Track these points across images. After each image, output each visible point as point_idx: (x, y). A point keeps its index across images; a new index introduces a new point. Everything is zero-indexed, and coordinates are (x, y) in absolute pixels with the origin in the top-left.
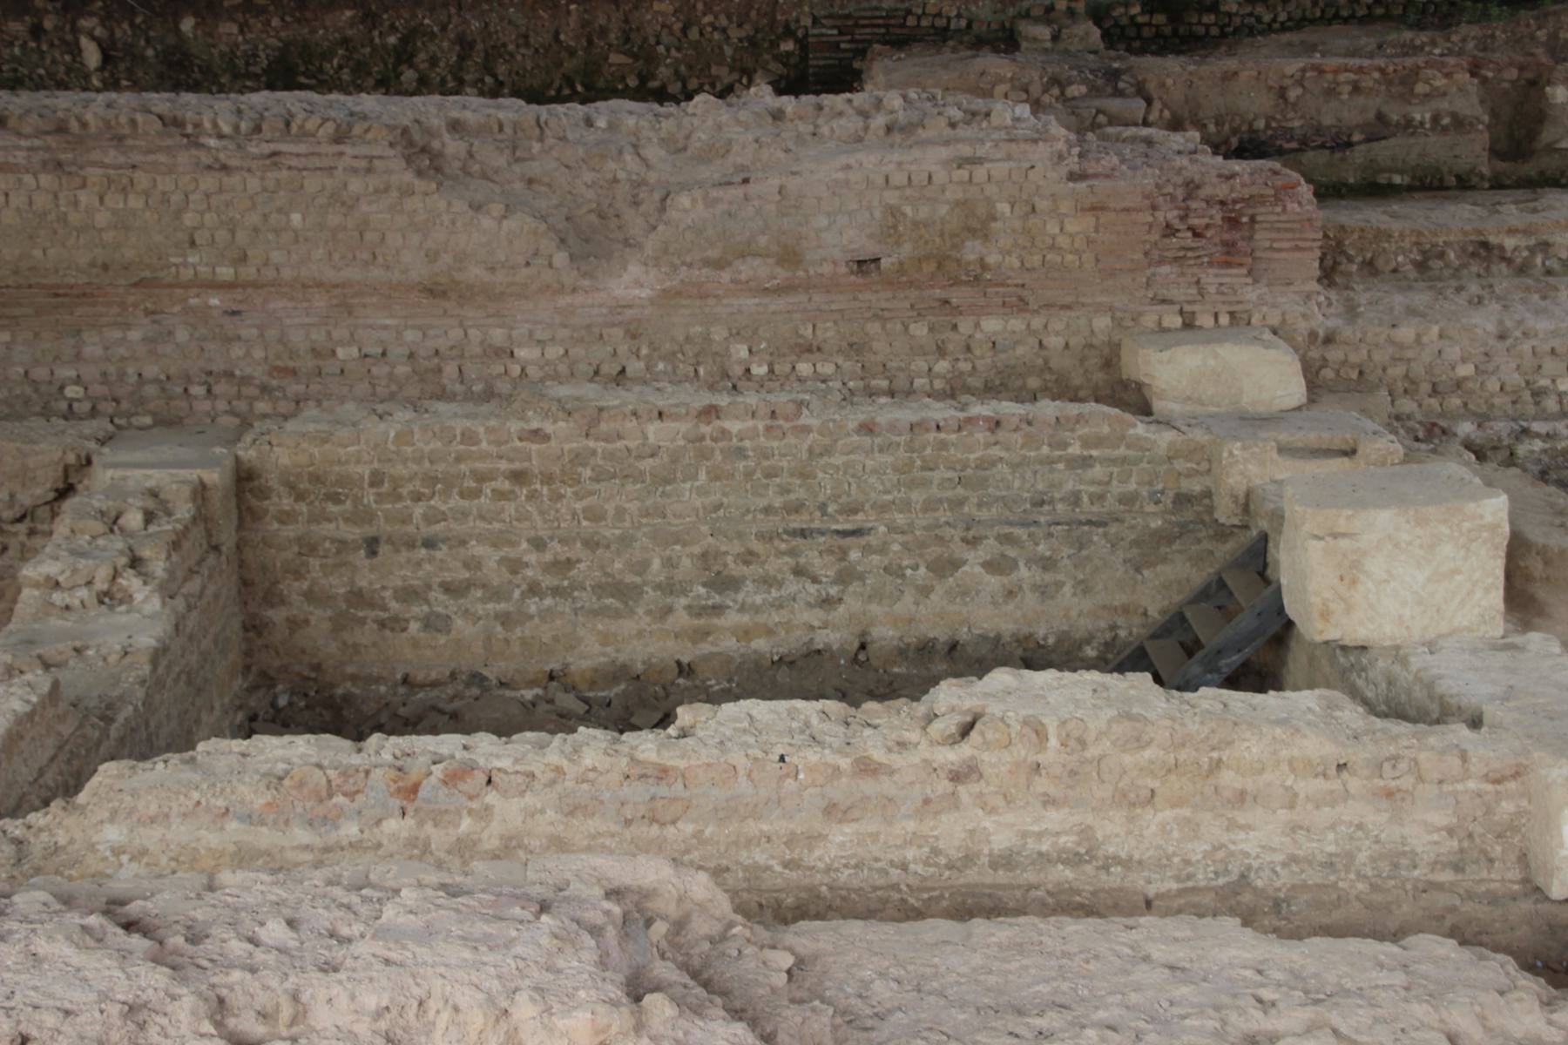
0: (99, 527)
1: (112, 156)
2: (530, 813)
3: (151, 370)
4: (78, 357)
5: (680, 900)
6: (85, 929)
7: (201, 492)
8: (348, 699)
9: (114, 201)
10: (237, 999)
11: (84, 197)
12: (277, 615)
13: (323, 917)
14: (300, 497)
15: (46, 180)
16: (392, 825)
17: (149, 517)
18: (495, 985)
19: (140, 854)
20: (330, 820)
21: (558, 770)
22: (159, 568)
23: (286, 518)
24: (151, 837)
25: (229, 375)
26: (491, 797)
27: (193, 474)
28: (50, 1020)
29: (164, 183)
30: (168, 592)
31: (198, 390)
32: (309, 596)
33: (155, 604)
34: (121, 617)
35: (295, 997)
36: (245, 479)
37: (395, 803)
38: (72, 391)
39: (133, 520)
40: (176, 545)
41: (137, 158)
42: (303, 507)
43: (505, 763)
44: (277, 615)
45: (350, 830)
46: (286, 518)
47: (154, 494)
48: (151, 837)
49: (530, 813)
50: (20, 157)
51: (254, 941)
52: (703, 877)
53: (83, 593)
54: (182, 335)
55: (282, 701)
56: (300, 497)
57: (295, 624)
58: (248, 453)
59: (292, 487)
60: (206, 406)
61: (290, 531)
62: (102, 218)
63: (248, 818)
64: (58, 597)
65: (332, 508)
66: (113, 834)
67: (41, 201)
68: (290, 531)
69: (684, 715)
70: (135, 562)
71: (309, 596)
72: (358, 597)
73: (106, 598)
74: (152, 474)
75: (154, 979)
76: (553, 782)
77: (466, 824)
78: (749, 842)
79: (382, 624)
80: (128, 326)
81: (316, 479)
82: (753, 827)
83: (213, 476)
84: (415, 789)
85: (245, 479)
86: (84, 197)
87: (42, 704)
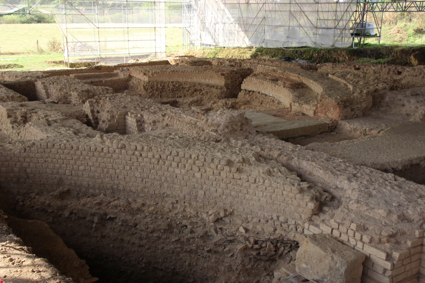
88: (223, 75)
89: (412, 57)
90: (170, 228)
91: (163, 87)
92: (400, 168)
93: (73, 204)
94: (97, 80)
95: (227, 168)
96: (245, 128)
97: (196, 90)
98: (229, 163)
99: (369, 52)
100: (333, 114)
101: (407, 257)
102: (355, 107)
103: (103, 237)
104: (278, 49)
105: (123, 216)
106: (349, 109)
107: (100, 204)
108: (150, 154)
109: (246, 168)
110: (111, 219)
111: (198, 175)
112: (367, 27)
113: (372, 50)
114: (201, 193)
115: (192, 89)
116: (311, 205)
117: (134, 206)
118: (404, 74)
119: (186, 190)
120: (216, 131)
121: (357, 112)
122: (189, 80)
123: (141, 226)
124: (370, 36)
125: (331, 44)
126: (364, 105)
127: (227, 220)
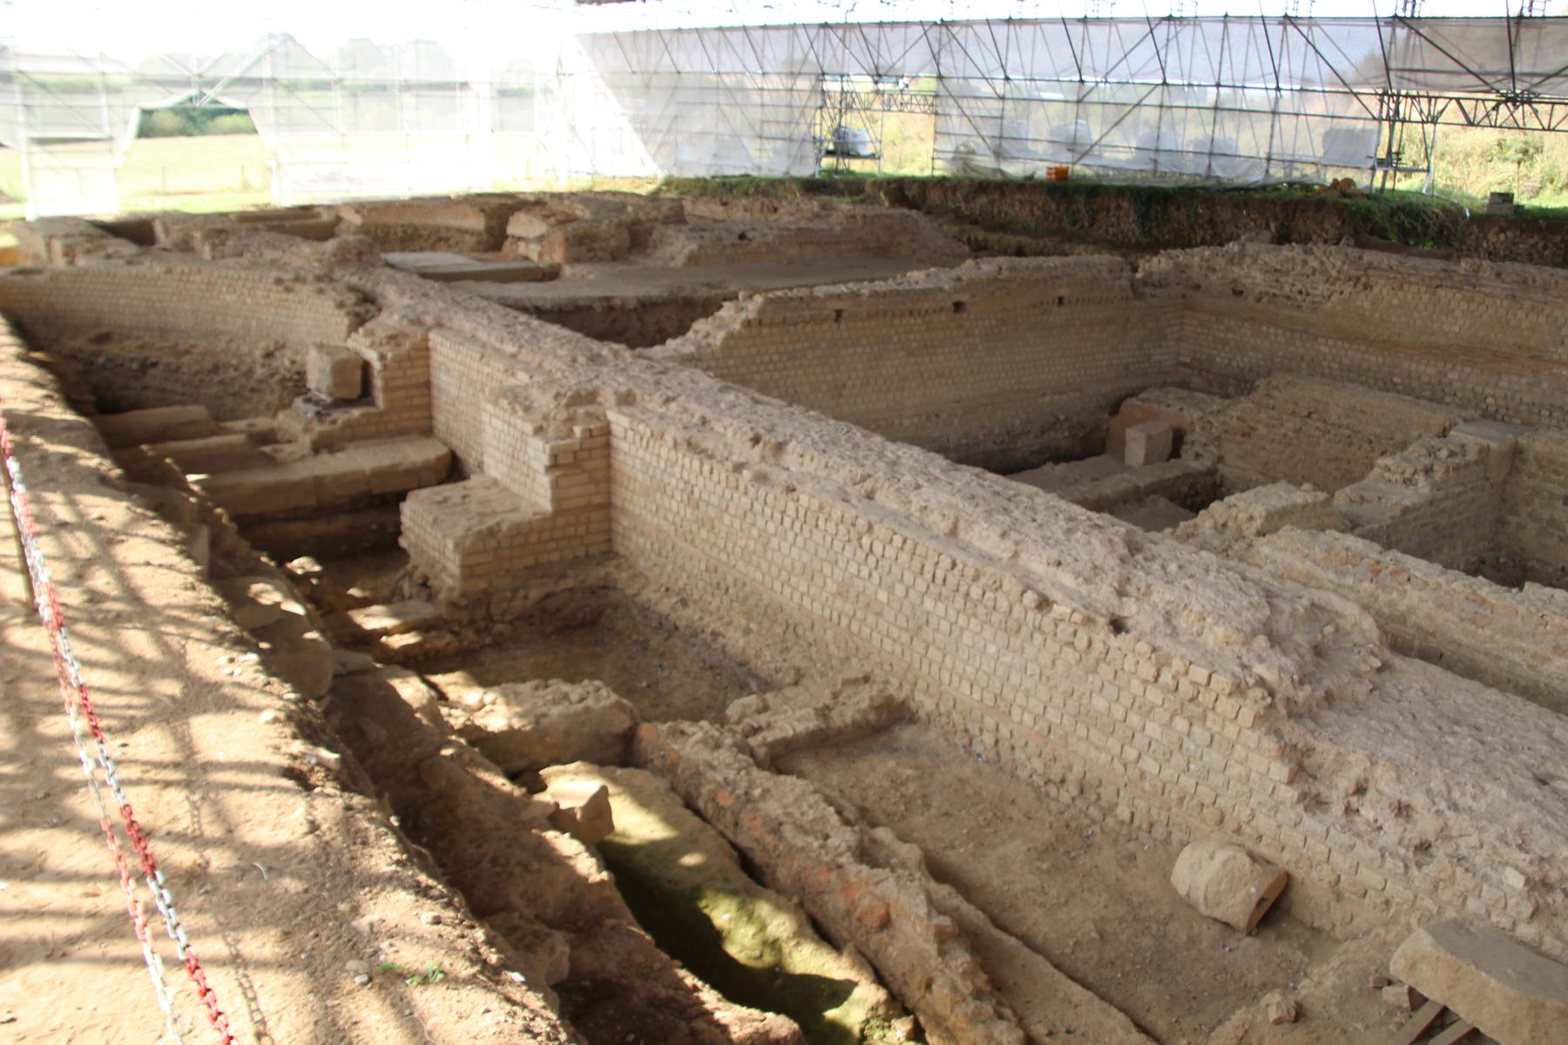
0: (1424, 452)
1: (1539, 296)
2: (1422, 600)
3: (1527, 399)
4: (1497, 385)
5: (1355, 624)
6: (1110, 541)
7: (1484, 451)
8: (1532, 569)
9: (1533, 317)
10: (1135, 581)
11: (1520, 314)
12: (1513, 520)
13: (1193, 569)
14: (1541, 467)
15: (1505, 303)
16: (1366, 584)
17: (1452, 454)
18: (1209, 609)
19: (1274, 562)
20: (1344, 574)
21: (1439, 585)
22: (1438, 474)
23: (1531, 475)
24: (1279, 556)
25: (1561, 408)
26: (1408, 587)
27: (1485, 442)
28: (1070, 560)
29: (1557, 313)
30: (1436, 486)
31: (1545, 413)
32: (1530, 515)
33: (1427, 490)
34: (1409, 491)
35: (1148, 587)
36: (1517, 452)
37: (1369, 575)
38: (1490, 400)
39: (1444, 453)
40: (1457, 468)
41: (1550, 299)
42: (1541, 473)
43: (1418, 574)
44: (1513, 520)
45: (1349, 580)
46: (1531, 475)
47: (1463, 446)
48: (1279, 556)
49: (1422, 600)
50: (1498, 292)
51: (1163, 567)
52: (1370, 620)
53: (1398, 476)
54: (1545, 385)
55: (1502, 560)
56: (1541, 467)
57: (1520, 527)
58: (1523, 441)
59: (1538, 462)
60: (1547, 421)
61: (1531, 482)
62: (1525, 324)
63: (1314, 562)
64: (1387, 475)
65: (1554, 477)
66: (1266, 550)
67: (1501, 312)
68: (1531, 482)
69: (1527, 585)
70: (1428, 471)
71: (1530, 515)
72: (1552, 522)
73: (1407, 482)
74: (1471, 438)
75: (1113, 562)
76: (1435, 590)
77: (1395, 595)
78: (1514, 650)
79: (1561, 539)
80: (1522, 376)
81: (1551, 461)
82: (1518, 643)
83: (1494, 445)
84: (1377, 573)
85: (1517, 452)
86: (1520, 314)
87: (1315, 504)
88: (482, 210)
89: (882, 195)
90: (216, 368)
91: (387, 235)
92: (548, 306)
93: (111, 349)
94: (276, 223)
95: (274, 288)
96: (365, 258)
97: (440, 240)
98: (279, 281)
99: (841, 186)
100: (558, 256)
101: (399, 361)
102: (596, 245)
103: (145, 388)
104: (698, 180)
105: (166, 359)
106: (584, 249)
107: (142, 347)
108: (198, 279)
109: (298, 287)
110: (154, 365)
111: (249, 300)
112: (850, 139)
113: (847, 183)
114: (254, 323)
115: (433, 238)
116: (346, 321)
117: (182, 347)
118: (781, 210)
119: (239, 322)
120: (320, 261)
121: (600, 254)
122: (431, 222)
123: (185, 370)
124: (858, 156)
125: (784, 169)
126: (613, 243)
127: (278, 354)
